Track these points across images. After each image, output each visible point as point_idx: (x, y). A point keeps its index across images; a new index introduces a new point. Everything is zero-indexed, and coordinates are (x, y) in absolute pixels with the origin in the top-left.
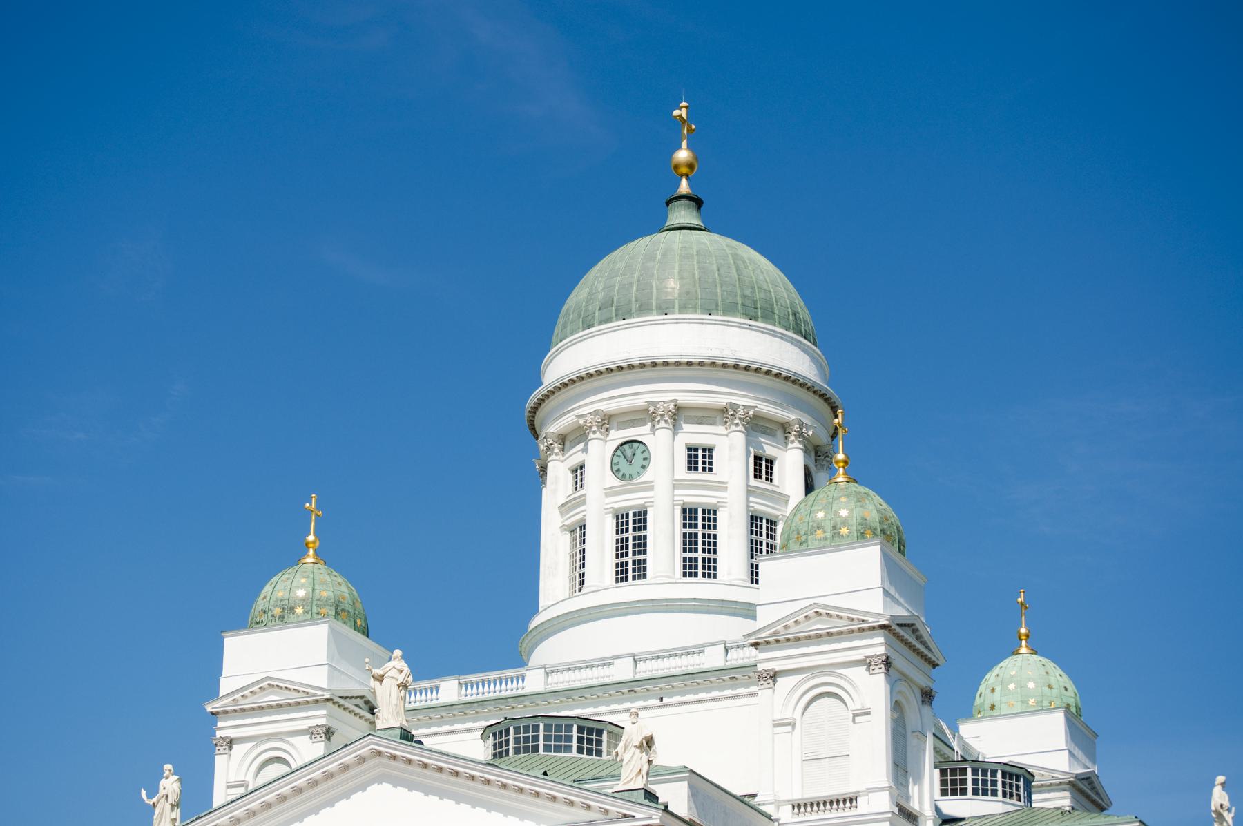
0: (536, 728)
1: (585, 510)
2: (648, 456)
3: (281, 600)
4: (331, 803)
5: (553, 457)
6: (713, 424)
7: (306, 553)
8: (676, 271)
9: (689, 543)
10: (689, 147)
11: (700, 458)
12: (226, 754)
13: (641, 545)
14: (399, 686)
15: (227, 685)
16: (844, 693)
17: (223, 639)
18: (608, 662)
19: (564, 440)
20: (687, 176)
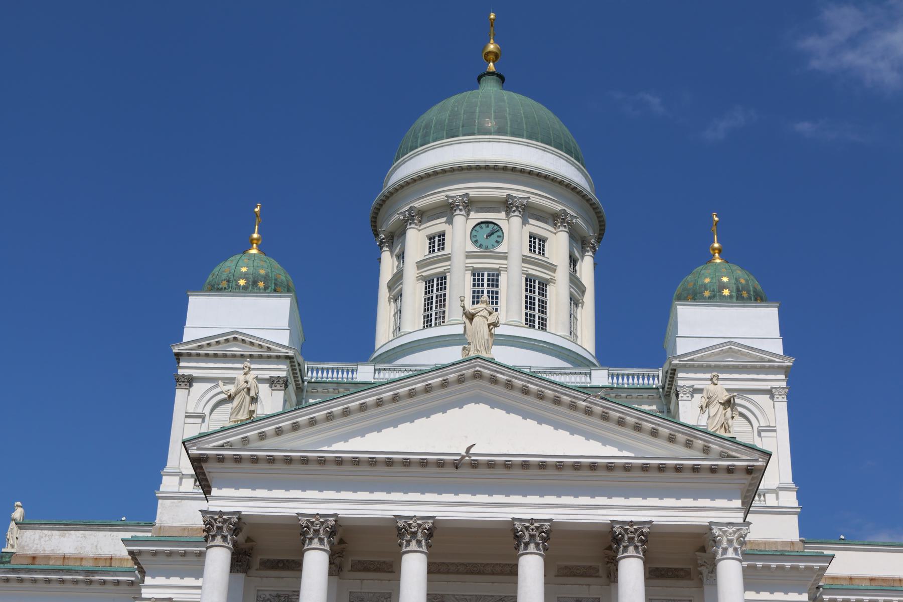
2: (501, 235)
4: (427, 414)
5: (413, 226)
6: (546, 223)
7: (251, 247)
8: (522, 112)
9: (529, 303)
10: (495, 42)
11: (537, 243)
12: (187, 389)
14: (489, 325)
15: (188, 335)
16: (749, 413)
17: (188, 297)
19: (424, 215)
20: (494, 62)
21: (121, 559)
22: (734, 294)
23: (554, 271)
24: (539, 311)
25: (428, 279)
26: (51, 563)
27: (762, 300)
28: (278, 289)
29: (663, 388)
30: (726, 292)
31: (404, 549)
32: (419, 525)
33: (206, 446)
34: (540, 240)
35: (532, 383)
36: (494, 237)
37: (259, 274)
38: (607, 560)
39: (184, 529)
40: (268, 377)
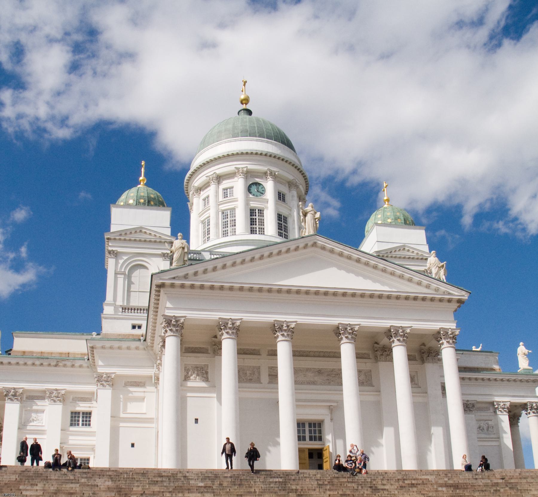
2: (263, 189)
3: (143, 197)
9: (280, 227)
13: (262, 222)
14: (315, 219)
15: (113, 229)
22: (403, 222)
24: (284, 230)
27: (415, 225)
33: (167, 278)
34: (283, 194)
35: (345, 250)
37: (151, 197)
38: (376, 349)
39: (120, 335)
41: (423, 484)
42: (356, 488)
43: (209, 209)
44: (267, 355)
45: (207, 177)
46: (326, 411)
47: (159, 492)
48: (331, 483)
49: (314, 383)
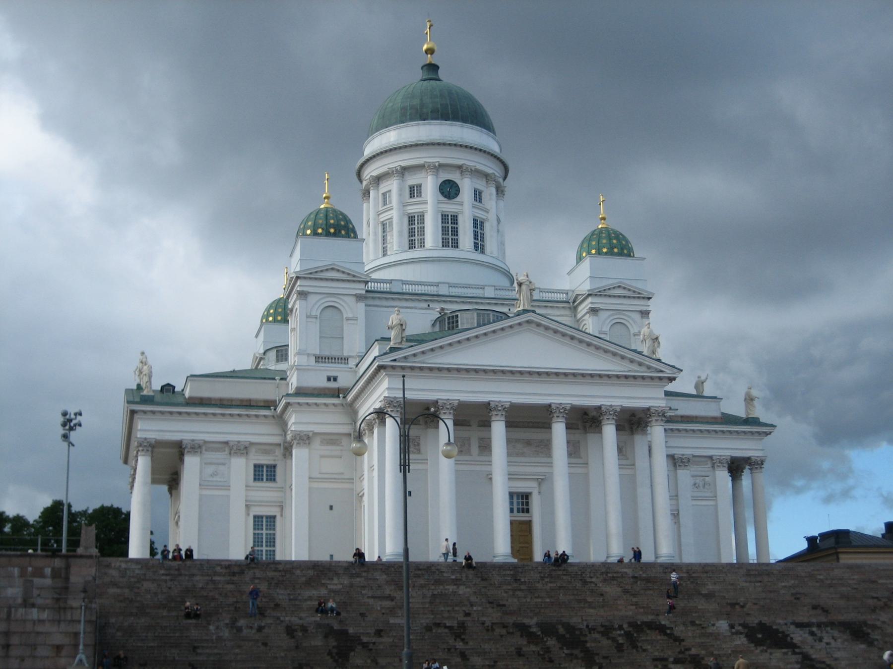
0: (488, 315)
1: (427, 208)
13: (455, 232)
14: (530, 290)
18: (482, 288)
21: (257, 401)
22: (620, 252)
23: (488, 212)
25: (410, 215)
26: (213, 402)
28: (352, 235)
29: (574, 302)
30: (616, 250)
31: (493, 418)
32: (502, 406)
34: (479, 192)
35: (560, 327)
36: (453, 191)
38: (585, 420)
39: (315, 389)
40: (354, 293)
41: (622, 577)
42: (570, 580)
43: (392, 209)
44: (478, 426)
45: (388, 168)
46: (534, 484)
47: (425, 584)
48: (550, 576)
49: (523, 455)
